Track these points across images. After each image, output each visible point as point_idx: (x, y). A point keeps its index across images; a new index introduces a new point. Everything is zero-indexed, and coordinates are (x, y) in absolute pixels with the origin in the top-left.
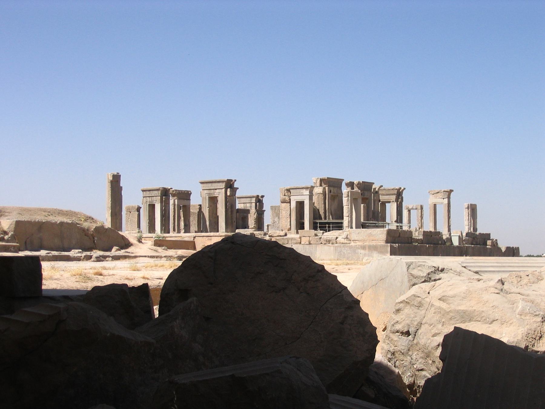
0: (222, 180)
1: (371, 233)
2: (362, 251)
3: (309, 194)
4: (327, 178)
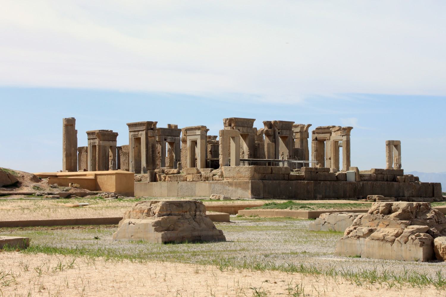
0: (143, 123)
2: (230, 188)
3: (200, 134)
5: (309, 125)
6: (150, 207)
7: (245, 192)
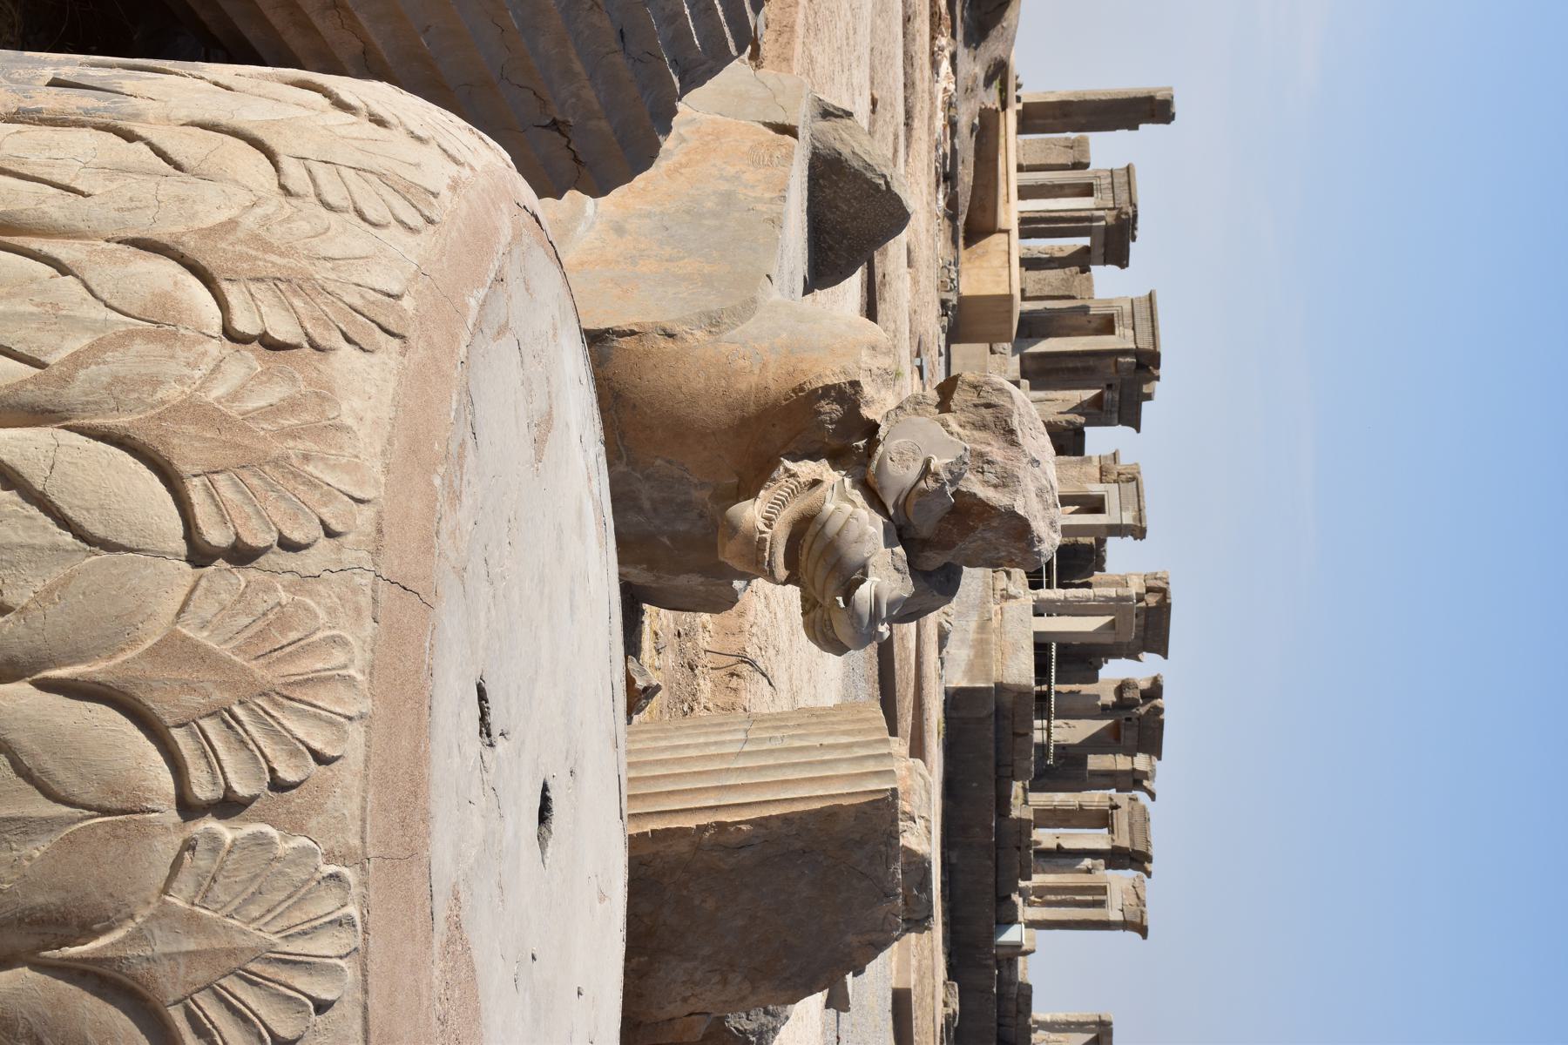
1: (1022, 651)
4: (1170, 604)
5: (1152, 796)
6: (916, 817)
7: (963, 669)
